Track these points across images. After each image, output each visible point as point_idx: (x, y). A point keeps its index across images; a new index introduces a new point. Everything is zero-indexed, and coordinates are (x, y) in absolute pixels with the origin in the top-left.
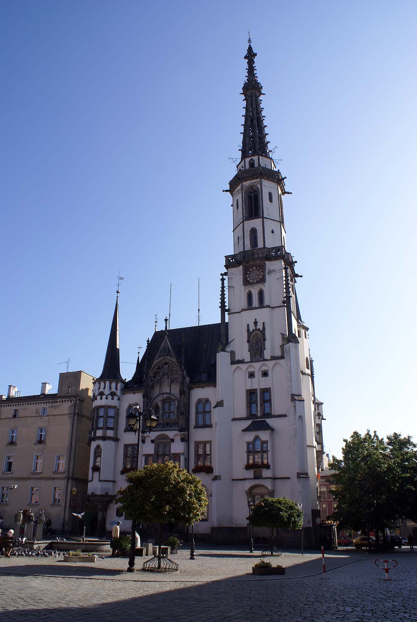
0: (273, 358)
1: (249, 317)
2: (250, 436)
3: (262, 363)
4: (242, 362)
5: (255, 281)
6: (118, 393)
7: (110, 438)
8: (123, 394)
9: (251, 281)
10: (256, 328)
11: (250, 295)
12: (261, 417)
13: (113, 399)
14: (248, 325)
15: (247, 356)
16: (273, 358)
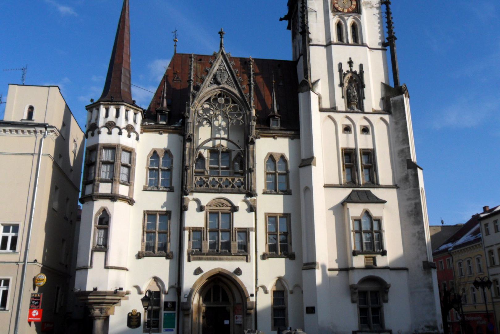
0: (375, 112)
1: (342, 54)
2: (356, 210)
3: (363, 115)
4: (334, 109)
5: (346, 10)
6: (138, 128)
7: (123, 199)
8: (141, 133)
9: (340, 9)
10: (351, 70)
11: (339, 26)
12: (365, 185)
13: (129, 136)
14: (340, 65)
15: (341, 104)
16: (375, 112)
